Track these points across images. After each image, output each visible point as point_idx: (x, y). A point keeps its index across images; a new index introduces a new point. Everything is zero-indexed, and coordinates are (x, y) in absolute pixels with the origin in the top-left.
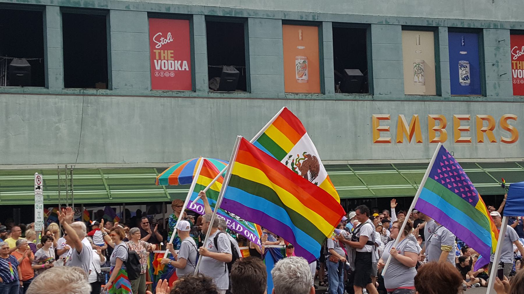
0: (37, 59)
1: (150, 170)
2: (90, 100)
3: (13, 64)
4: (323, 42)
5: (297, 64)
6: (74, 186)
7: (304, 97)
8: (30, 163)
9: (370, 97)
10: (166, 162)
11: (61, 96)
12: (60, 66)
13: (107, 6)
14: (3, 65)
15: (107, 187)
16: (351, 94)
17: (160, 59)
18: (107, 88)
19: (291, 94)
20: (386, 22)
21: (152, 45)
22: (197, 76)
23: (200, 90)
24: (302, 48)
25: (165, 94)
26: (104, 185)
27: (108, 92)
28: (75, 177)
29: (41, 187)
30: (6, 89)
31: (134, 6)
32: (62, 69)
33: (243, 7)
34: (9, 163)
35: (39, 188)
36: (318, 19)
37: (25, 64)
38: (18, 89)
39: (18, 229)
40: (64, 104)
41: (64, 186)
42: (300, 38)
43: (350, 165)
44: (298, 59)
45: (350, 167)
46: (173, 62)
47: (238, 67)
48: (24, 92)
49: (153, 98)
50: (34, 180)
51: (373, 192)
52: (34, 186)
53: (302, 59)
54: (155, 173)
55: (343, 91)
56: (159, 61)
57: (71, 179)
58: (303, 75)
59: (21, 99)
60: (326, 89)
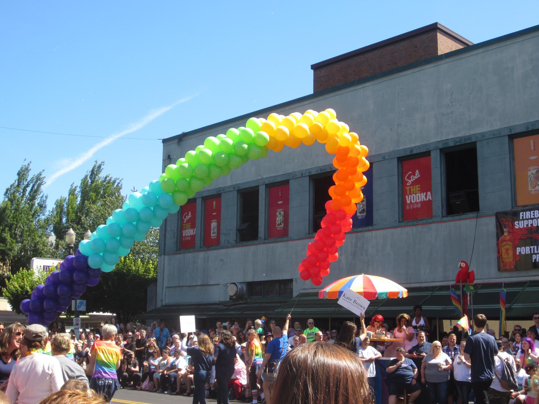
5: (530, 175)
23: (435, 216)
25: (408, 224)
27: (370, 228)
33: (472, 132)
42: (532, 148)
44: (530, 170)
53: (535, 169)
58: (536, 186)
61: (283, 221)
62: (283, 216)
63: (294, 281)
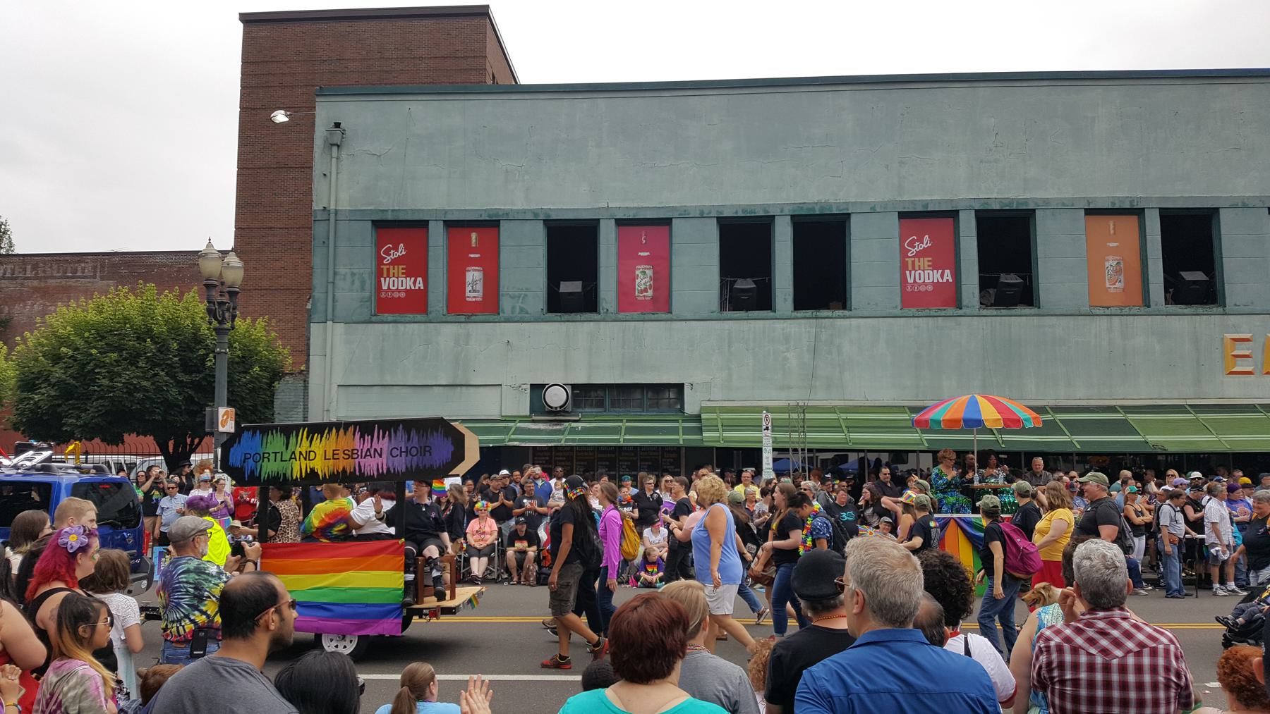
1: (900, 409)
2: (823, 325)
4: (1145, 236)
6: (807, 427)
7: (1119, 312)
9: (1220, 310)
10: (920, 399)
13: (848, 210)
15: (846, 432)
16: (1190, 306)
17: (914, 268)
18: (844, 308)
19: (1099, 308)
20: (1243, 205)
21: (904, 252)
22: (964, 288)
24: (1115, 244)
26: (841, 427)
28: (808, 416)
29: (770, 428)
31: (881, 206)
35: (767, 429)
36: (1137, 205)
41: (795, 427)
43: (1189, 405)
45: (1189, 409)
46: (931, 272)
47: (1021, 274)
49: (903, 320)
50: (762, 419)
51: (1226, 445)
52: (761, 426)
54: (907, 413)
55: (1176, 304)
56: (913, 272)
57: (804, 419)
60: (1151, 300)
62: (650, 277)
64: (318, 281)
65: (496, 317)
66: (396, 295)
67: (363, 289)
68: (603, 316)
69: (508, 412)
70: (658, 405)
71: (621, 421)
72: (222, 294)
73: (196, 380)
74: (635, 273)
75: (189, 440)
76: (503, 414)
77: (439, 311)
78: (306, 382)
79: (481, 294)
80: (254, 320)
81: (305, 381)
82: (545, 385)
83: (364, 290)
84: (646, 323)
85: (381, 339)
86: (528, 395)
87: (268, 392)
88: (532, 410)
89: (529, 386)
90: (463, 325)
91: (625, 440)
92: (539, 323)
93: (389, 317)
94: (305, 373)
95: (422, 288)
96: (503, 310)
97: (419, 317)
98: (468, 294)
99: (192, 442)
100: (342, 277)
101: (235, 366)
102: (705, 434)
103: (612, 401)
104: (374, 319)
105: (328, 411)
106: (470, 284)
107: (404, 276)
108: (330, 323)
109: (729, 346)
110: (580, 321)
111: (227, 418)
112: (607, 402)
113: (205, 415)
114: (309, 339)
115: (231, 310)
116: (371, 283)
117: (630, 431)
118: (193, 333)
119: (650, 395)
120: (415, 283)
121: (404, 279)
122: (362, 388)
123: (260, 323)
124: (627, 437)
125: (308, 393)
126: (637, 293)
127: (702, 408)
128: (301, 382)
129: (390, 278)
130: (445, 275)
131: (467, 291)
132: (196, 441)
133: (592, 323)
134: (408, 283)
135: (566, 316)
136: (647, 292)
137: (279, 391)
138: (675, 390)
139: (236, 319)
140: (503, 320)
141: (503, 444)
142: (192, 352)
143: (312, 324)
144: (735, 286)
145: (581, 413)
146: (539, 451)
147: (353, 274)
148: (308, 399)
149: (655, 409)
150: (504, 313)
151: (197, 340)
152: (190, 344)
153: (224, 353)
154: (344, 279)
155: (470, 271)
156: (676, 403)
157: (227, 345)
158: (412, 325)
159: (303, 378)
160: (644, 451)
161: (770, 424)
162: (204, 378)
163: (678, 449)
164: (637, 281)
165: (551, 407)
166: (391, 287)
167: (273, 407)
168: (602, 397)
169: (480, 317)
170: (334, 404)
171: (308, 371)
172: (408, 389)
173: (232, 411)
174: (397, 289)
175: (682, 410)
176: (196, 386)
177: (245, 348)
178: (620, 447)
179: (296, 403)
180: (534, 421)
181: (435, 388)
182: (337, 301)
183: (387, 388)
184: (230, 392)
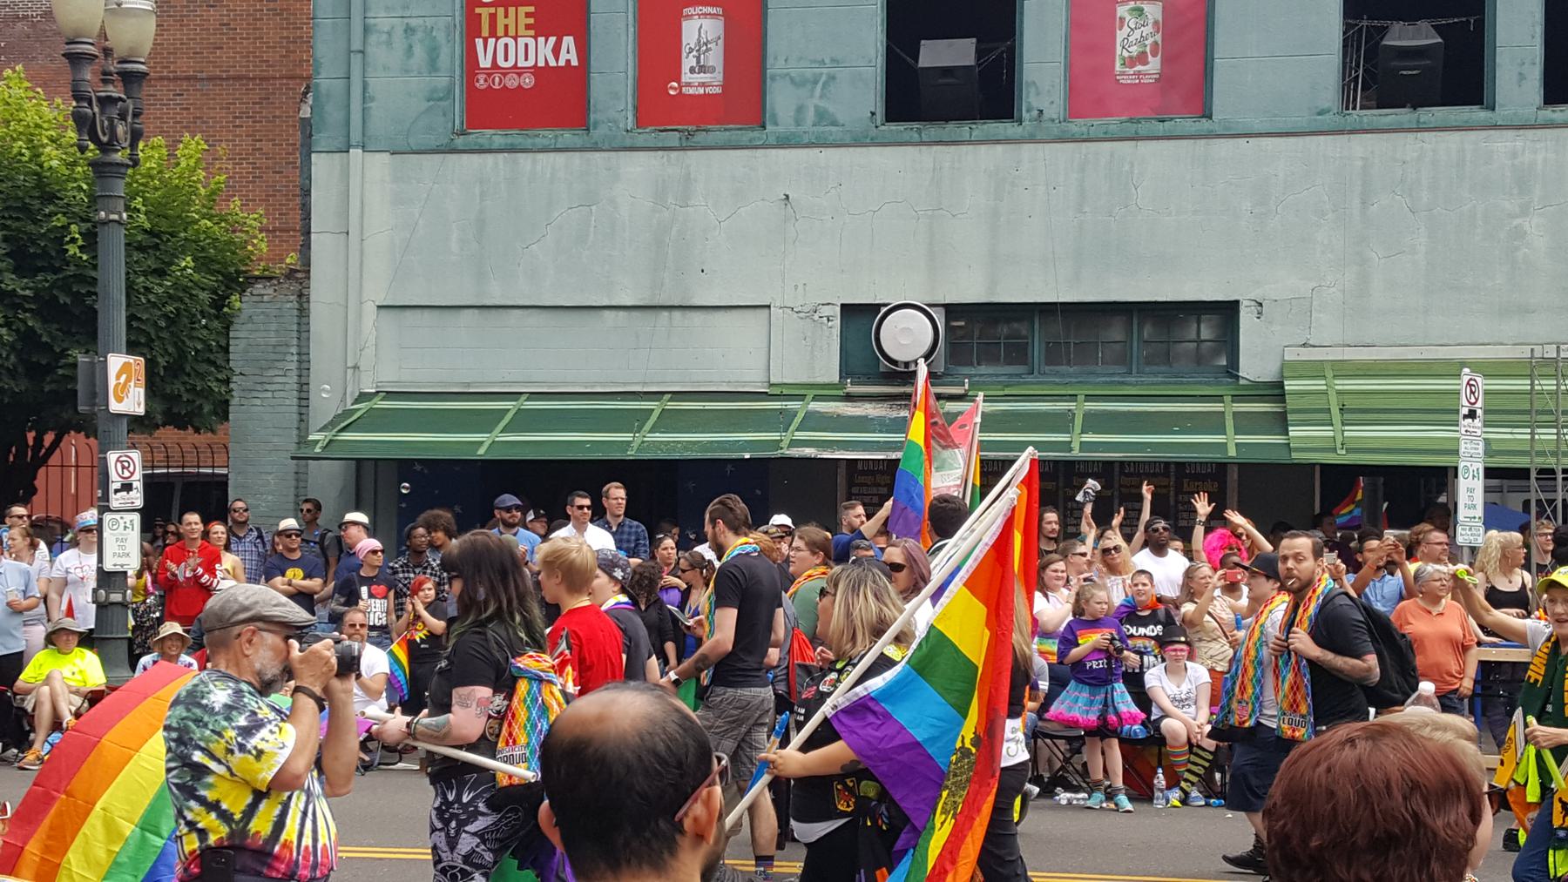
0: (1464, 19)
3: (1385, 42)
8: (1427, 342)
11: (1534, 131)
12: (1533, 37)
14: (1352, 46)
30: (1365, 119)
32: (1538, 48)
34: (1369, 341)
37: (1427, 38)
38: (1402, 115)
39: (1437, 537)
40: (1540, 157)
48: (1418, 122)
59: (1409, 145)
61: (1156, 43)
63: (1242, 308)
64: (326, 48)
65: (756, 134)
66: (512, 82)
67: (433, 65)
68: (1028, 128)
69: (788, 372)
70: (1167, 359)
71: (1073, 397)
72: (106, 78)
73: (45, 289)
74: (1115, 10)
75: (31, 436)
76: (773, 380)
77: (615, 122)
78: (303, 297)
79: (721, 77)
80: (173, 146)
81: (300, 296)
82: (878, 307)
83: (436, 70)
84: (1140, 143)
85: (477, 191)
86: (837, 331)
87: (216, 324)
88: (846, 371)
89: (838, 309)
90: (674, 154)
91: (1084, 446)
92: (864, 149)
93: (496, 137)
94: (299, 275)
95: (575, 63)
96: (774, 116)
97: (568, 137)
98: (686, 77)
99: (39, 440)
100: (384, 37)
101: (136, 256)
102: (1294, 432)
103: (1048, 350)
104: (460, 142)
105: (356, 367)
106: (691, 50)
107: (532, 32)
108: (356, 153)
109: (1363, 203)
110: (970, 142)
111: (128, 380)
112: (1037, 351)
113: (74, 379)
114: (307, 193)
115: (129, 119)
116: (453, 57)
117: (1094, 422)
118: (36, 174)
119: (1147, 331)
120: (556, 51)
121: (531, 42)
122: (436, 313)
123: (192, 146)
124: (1090, 438)
125: (309, 324)
126: (1118, 67)
127: (1284, 365)
128: (292, 297)
129: (498, 39)
130: (631, 30)
131: (685, 68)
132: (49, 438)
133: (999, 148)
134: (541, 52)
135: (932, 131)
136: (1145, 63)
137: (244, 317)
138: (1215, 318)
139: (141, 145)
140: (772, 140)
141: (778, 454)
142: (35, 222)
143: (313, 155)
144: (1385, 42)
145: (970, 376)
146: (863, 473)
147: (409, 30)
148: (309, 339)
149: (1163, 368)
150: (776, 124)
151: (47, 191)
152: (27, 201)
153: (118, 222)
154: (389, 43)
155: (689, 17)
156: (1216, 353)
157: (121, 205)
158: (552, 155)
159: (295, 287)
160: (1130, 475)
161: (1479, 404)
162: (65, 286)
163: (1222, 468)
164: (1120, 35)
165: (895, 362)
166: (501, 62)
167: (228, 360)
168: (1026, 338)
169: (717, 135)
170: (370, 351)
171: (309, 271)
172: (544, 315)
173: (138, 363)
174: (515, 66)
175: (1232, 370)
176: (46, 306)
177: (156, 211)
178: (1070, 464)
179: (279, 349)
180: (849, 398)
181: (607, 313)
182: (372, 99)
183: (493, 311)
184: (131, 318)
